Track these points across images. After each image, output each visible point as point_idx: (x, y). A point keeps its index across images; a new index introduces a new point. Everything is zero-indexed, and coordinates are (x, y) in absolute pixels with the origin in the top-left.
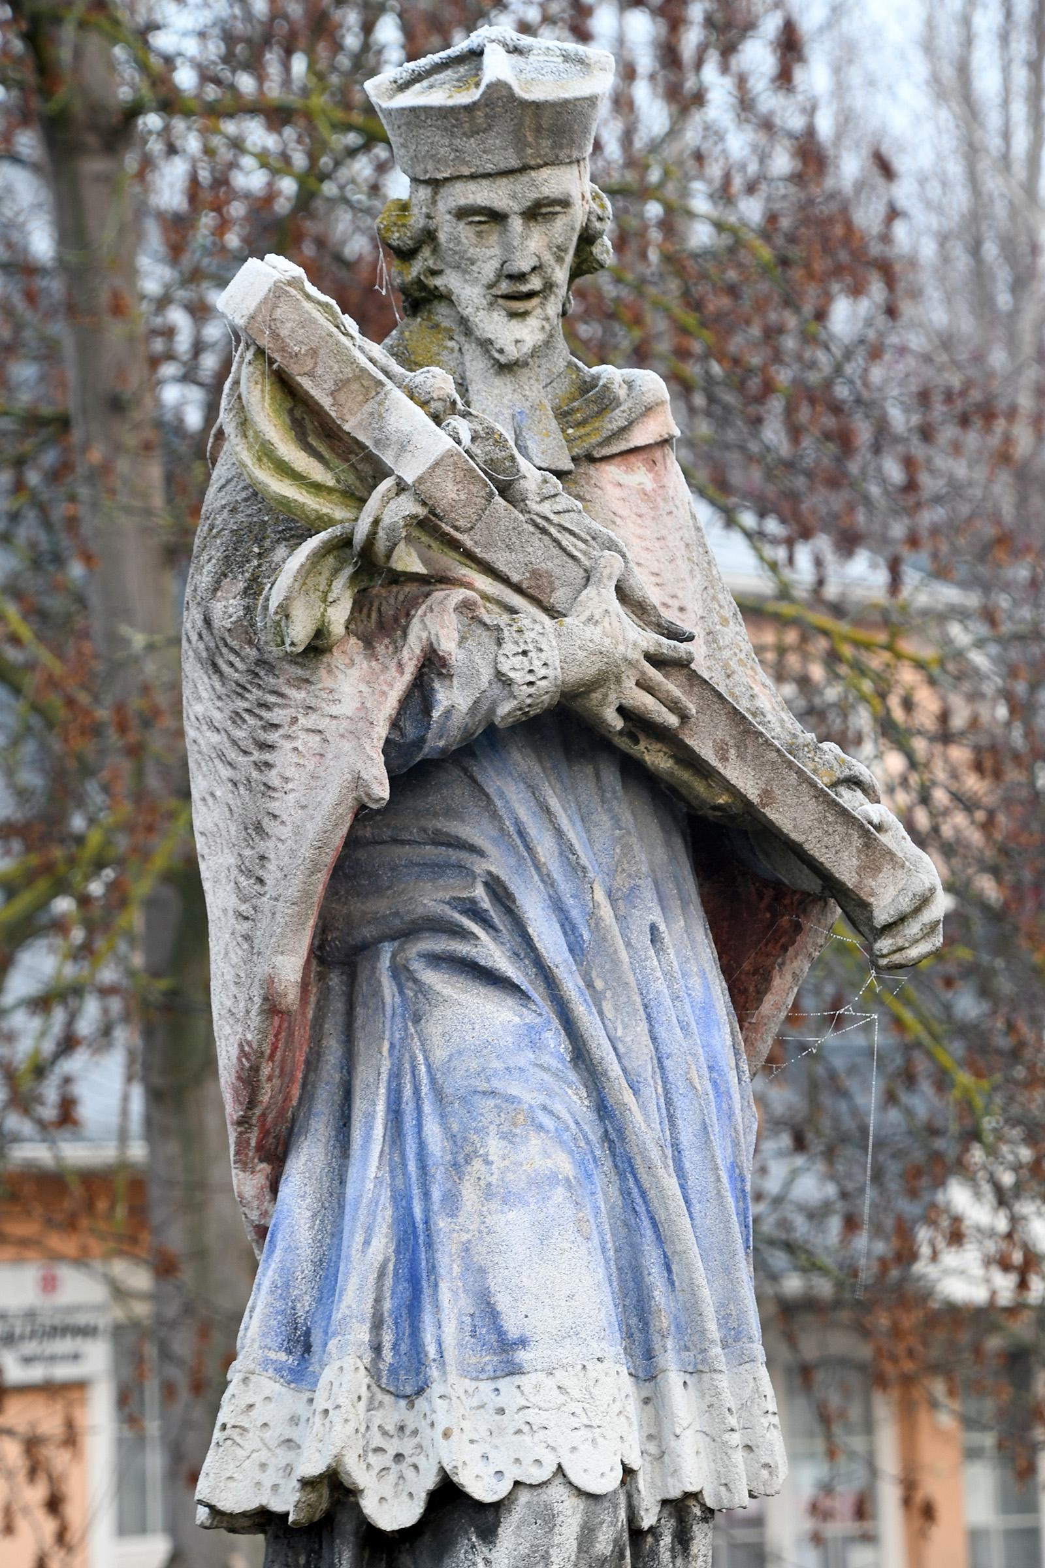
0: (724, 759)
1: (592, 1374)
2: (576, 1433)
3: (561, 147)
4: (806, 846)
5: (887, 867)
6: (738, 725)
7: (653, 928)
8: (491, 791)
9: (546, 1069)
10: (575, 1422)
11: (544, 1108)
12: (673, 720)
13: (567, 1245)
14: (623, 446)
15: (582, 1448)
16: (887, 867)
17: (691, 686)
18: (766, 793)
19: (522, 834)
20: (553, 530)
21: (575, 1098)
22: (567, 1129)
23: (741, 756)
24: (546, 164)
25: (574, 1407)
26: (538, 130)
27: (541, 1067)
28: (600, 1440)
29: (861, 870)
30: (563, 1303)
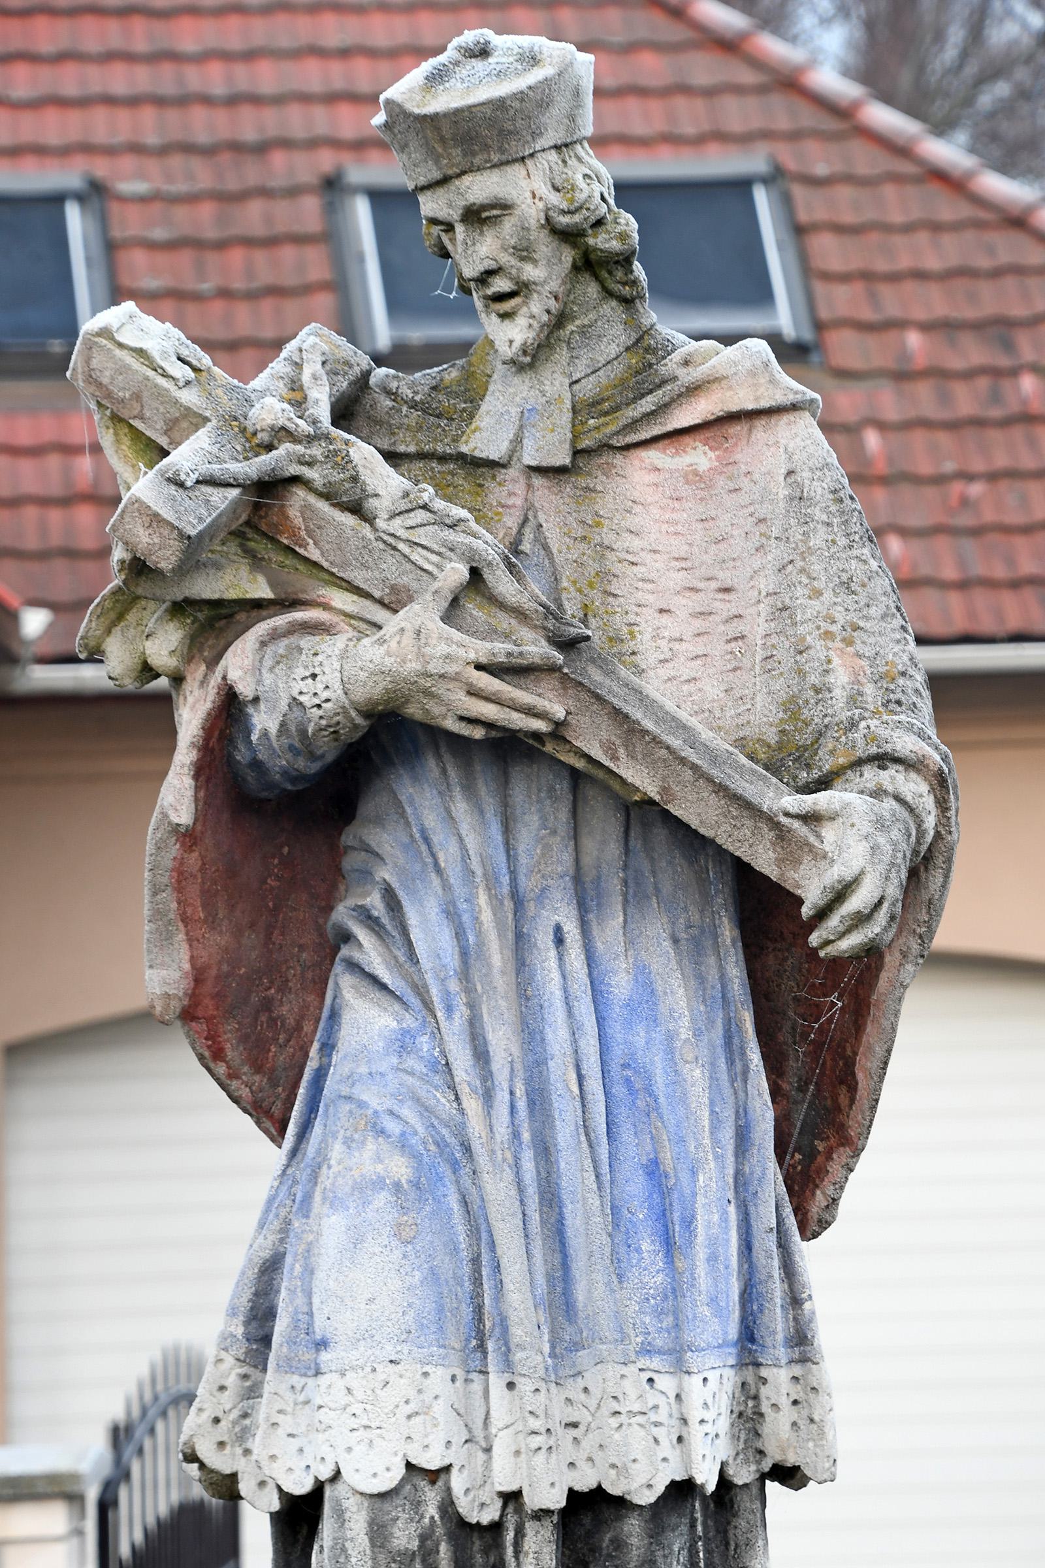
0: (615, 758)
1: (381, 1376)
2: (355, 1434)
3: (474, 154)
4: (719, 841)
5: (807, 859)
6: (621, 725)
7: (558, 929)
8: (403, 798)
9: (412, 1074)
10: (354, 1423)
11: (391, 1113)
12: (540, 726)
13: (377, 1250)
14: (657, 430)
15: (357, 1449)
16: (807, 859)
17: (565, 688)
18: (664, 790)
19: (427, 840)
20: (401, 546)
21: (443, 1100)
22: (416, 1133)
23: (631, 756)
24: (464, 173)
25: (357, 1408)
26: (443, 140)
27: (405, 1071)
28: (378, 1442)
29: (780, 862)
30: (363, 1306)
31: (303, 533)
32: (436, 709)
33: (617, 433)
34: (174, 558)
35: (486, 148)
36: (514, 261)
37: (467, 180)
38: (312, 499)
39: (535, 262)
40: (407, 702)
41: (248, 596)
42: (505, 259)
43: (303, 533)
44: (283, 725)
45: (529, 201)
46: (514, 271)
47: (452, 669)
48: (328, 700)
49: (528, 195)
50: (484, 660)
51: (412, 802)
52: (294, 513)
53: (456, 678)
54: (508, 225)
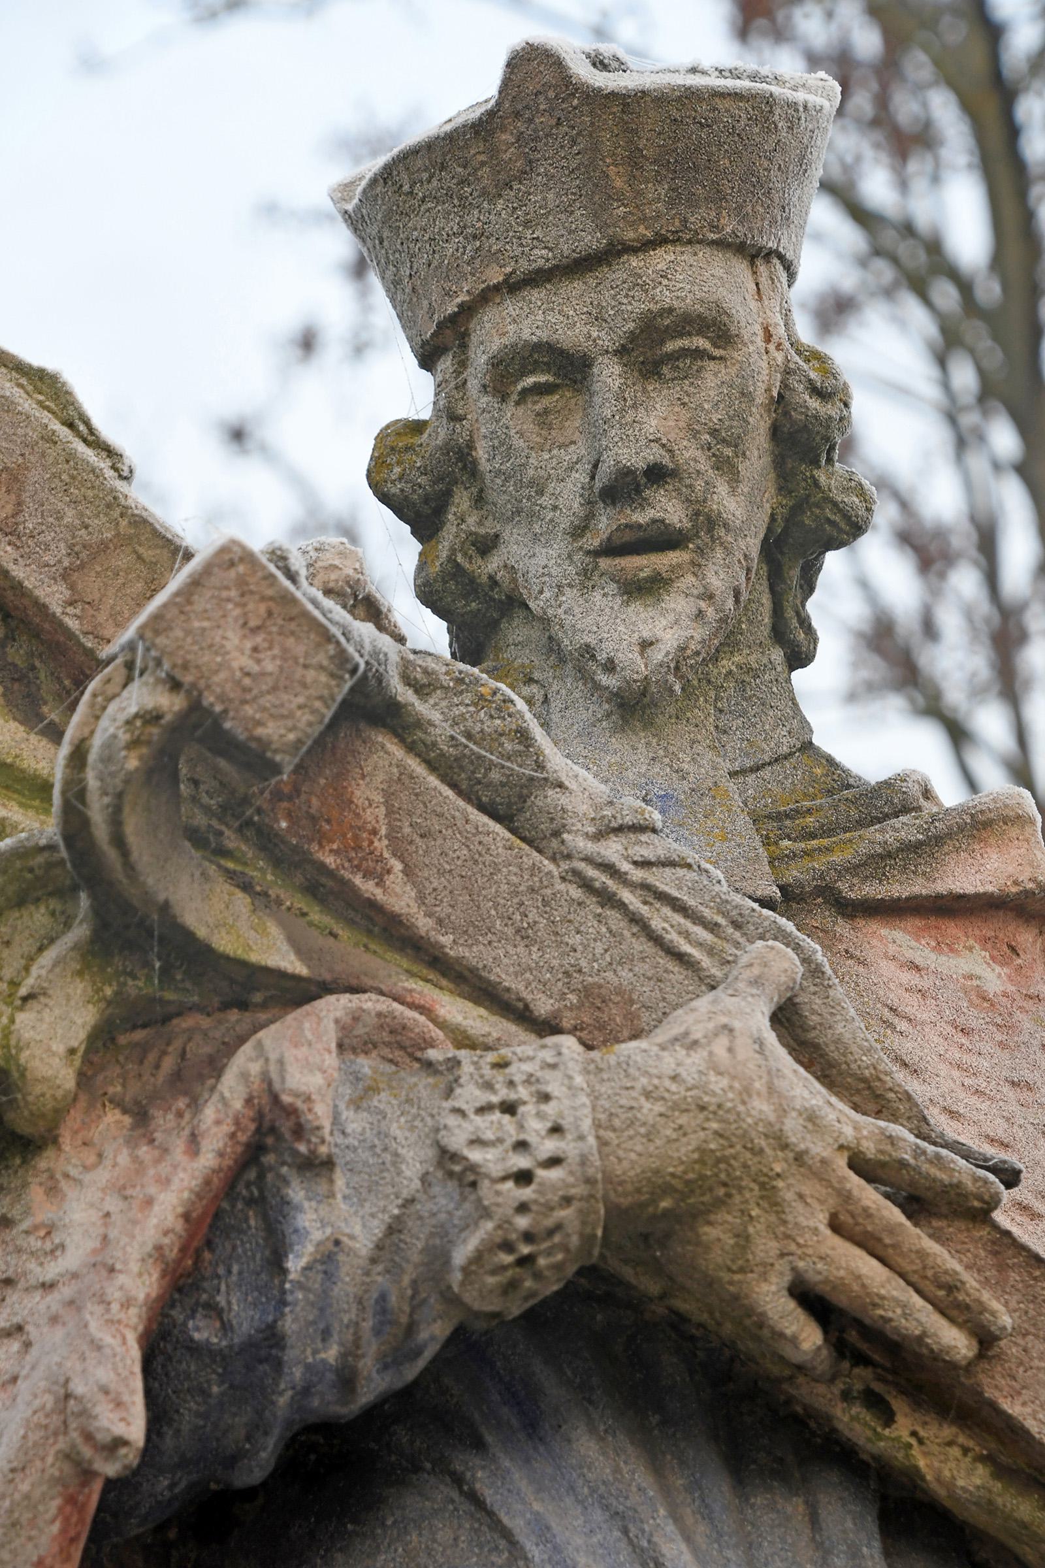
3: (693, 203)
8: (516, 1524)
12: (955, 1341)
14: (918, 887)
17: (1002, 1268)
20: (626, 896)
24: (660, 241)
26: (634, 160)
31: (381, 845)
32: (765, 1247)
33: (853, 869)
34: (305, 717)
35: (718, 198)
36: (704, 465)
37: (661, 258)
38: (415, 766)
39: (734, 479)
40: (720, 1203)
41: (254, 958)
42: (691, 455)
43: (381, 845)
44: (394, 1229)
45: (759, 341)
46: (699, 485)
47: (819, 1148)
48: (554, 1161)
49: (758, 329)
50: (870, 1149)
51: (543, 1532)
52: (368, 795)
53: (820, 1173)
54: (712, 381)
